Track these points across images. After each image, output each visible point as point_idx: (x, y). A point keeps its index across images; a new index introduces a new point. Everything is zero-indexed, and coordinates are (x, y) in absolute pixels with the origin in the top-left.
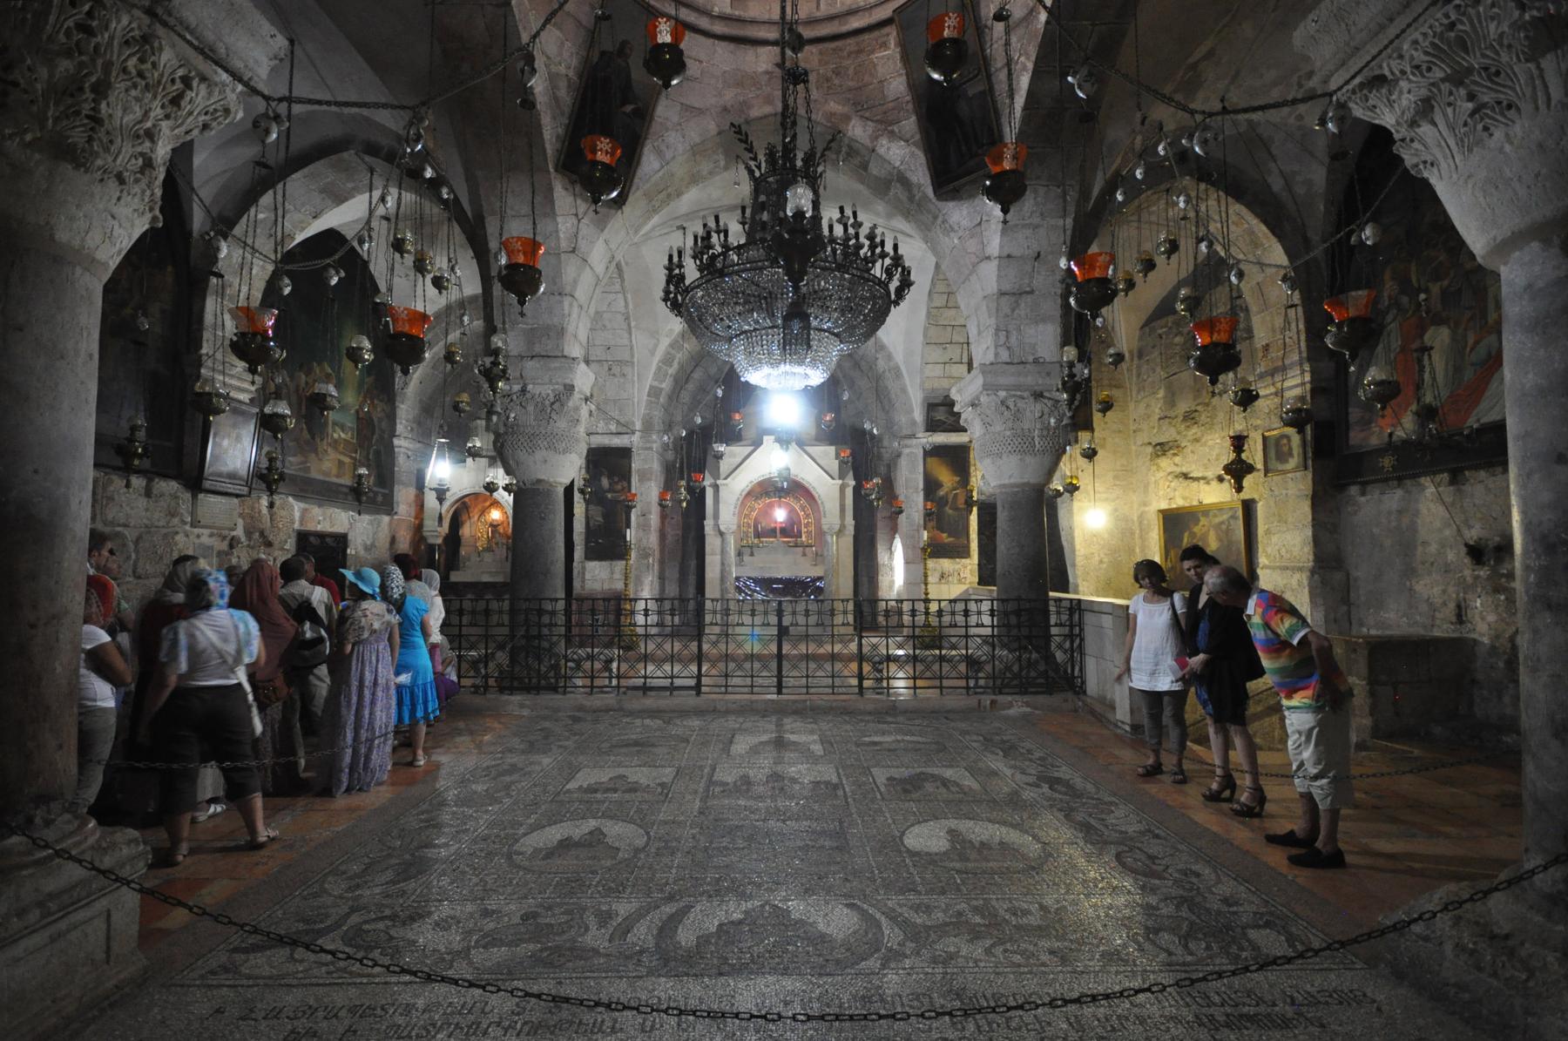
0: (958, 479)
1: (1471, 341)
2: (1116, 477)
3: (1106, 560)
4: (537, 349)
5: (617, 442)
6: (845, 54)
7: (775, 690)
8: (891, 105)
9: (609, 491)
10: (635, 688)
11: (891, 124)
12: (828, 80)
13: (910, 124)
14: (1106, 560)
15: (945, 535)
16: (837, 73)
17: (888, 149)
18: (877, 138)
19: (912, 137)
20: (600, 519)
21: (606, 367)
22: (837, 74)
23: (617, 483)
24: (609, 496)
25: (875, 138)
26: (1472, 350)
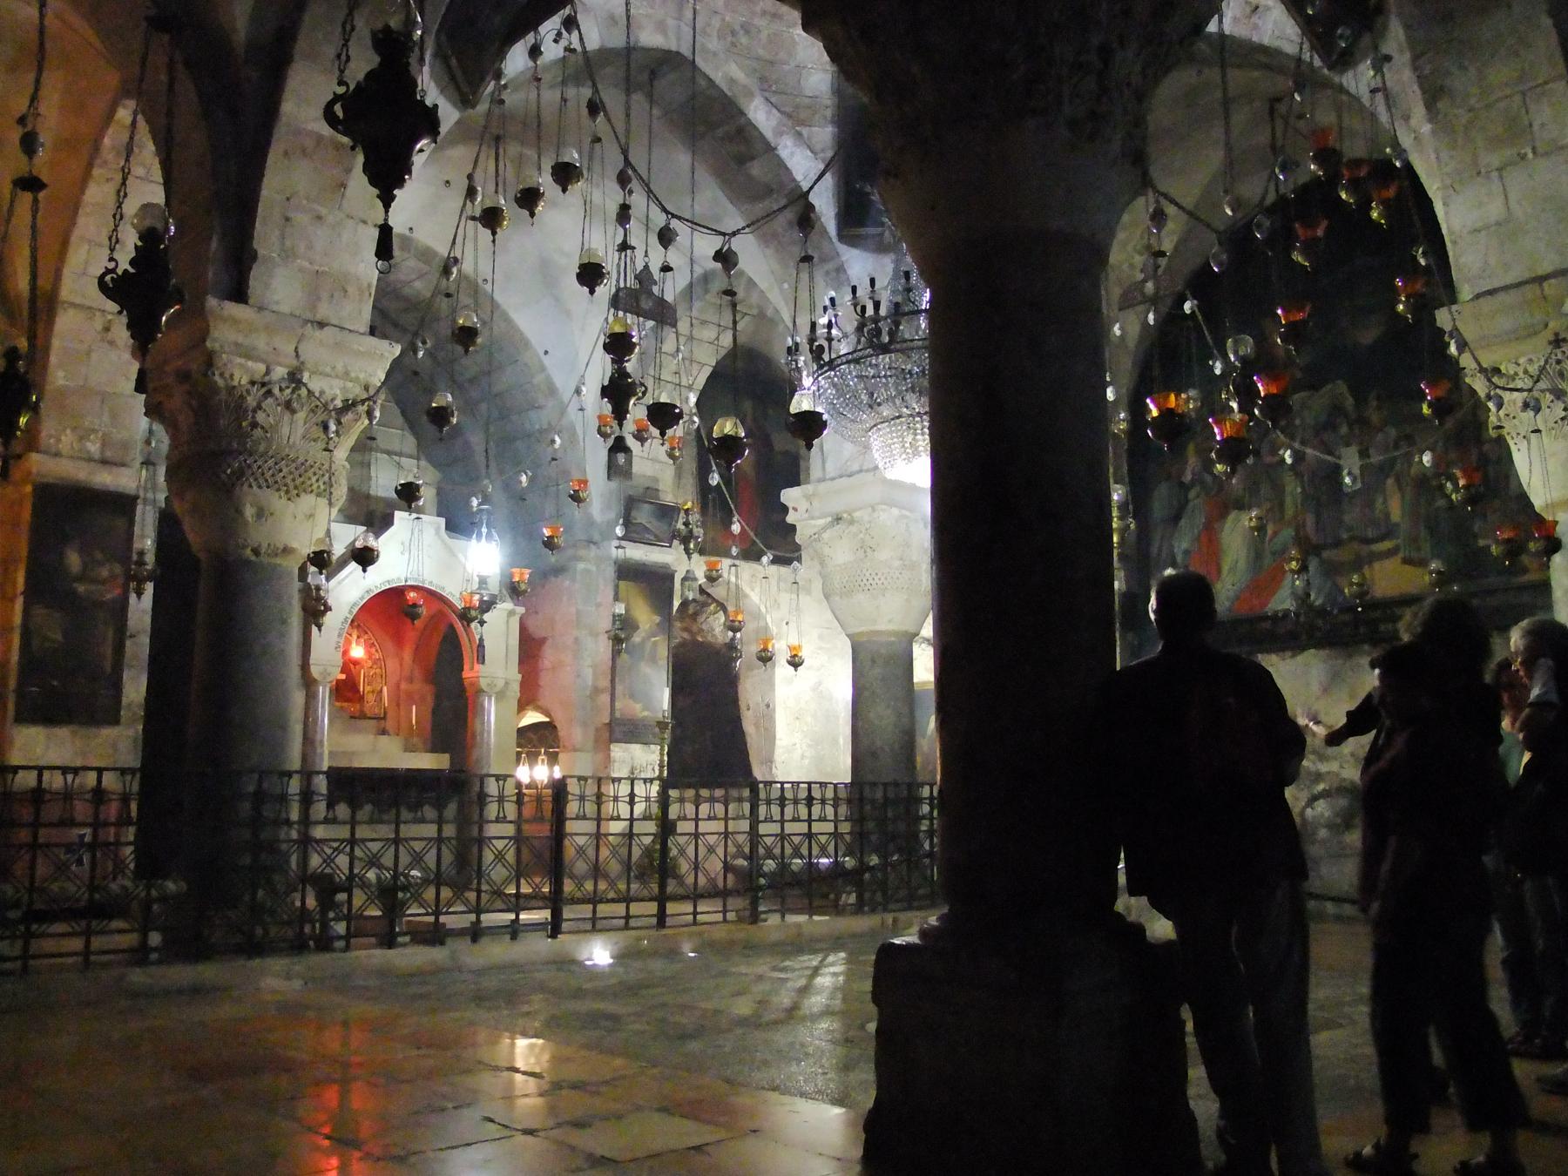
0: (657, 619)
1: (1270, 532)
2: (821, 637)
3: (807, 754)
4: (324, 311)
5: (105, 479)
6: (758, 9)
7: (654, 921)
8: (807, 101)
9: (81, 578)
10: (461, 933)
11: (803, 123)
12: (733, 33)
13: (825, 135)
14: (807, 754)
15: (638, 706)
16: (746, 28)
17: (792, 154)
18: (781, 134)
19: (823, 151)
20: (59, 637)
21: (98, 324)
22: (747, 32)
23: (101, 564)
24: (81, 588)
25: (779, 133)
26: (1271, 540)
